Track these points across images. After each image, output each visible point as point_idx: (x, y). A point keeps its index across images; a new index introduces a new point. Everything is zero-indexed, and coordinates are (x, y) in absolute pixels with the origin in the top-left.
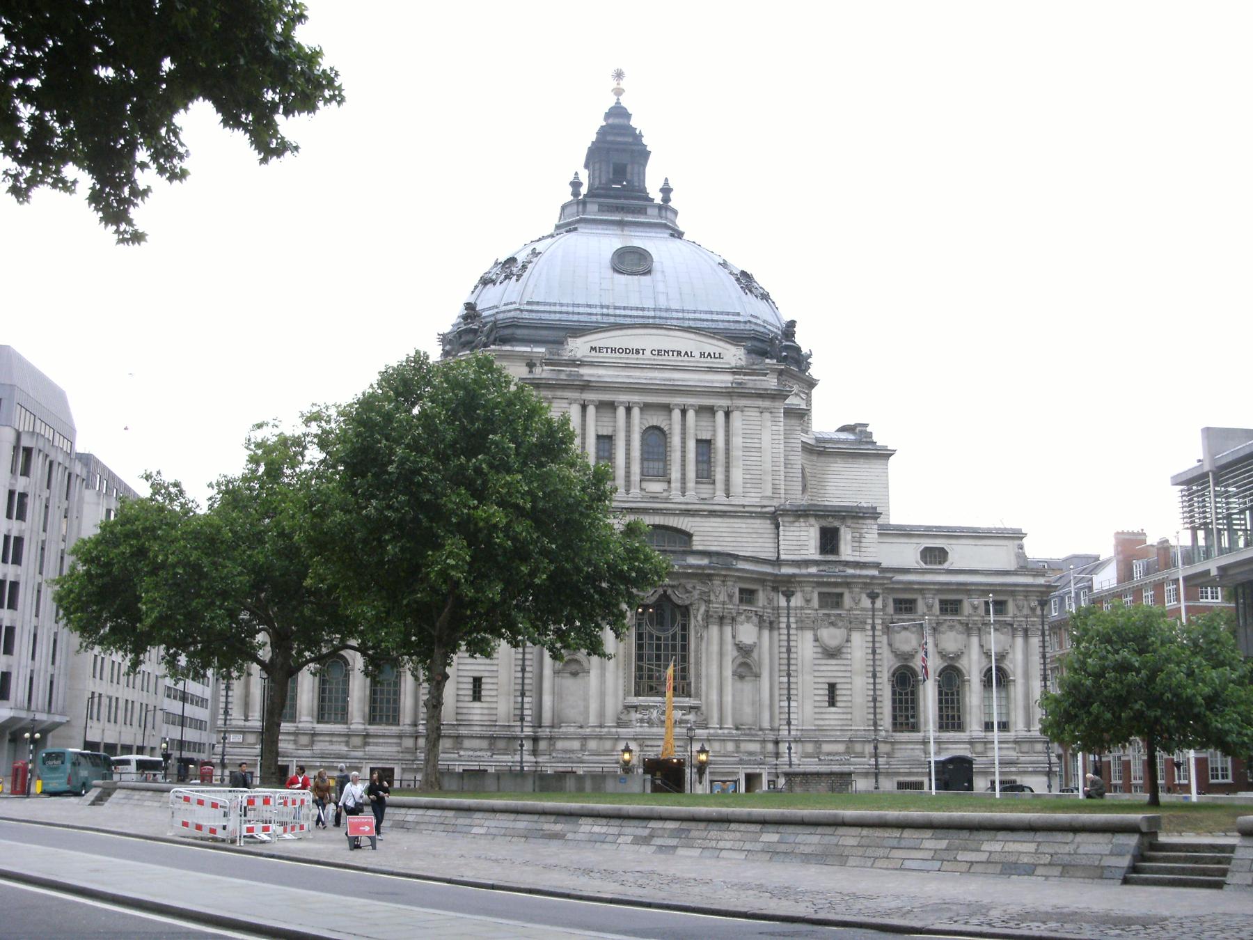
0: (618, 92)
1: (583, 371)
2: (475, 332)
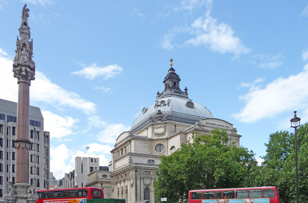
0: (171, 65)
1: (205, 128)
2: (162, 117)
